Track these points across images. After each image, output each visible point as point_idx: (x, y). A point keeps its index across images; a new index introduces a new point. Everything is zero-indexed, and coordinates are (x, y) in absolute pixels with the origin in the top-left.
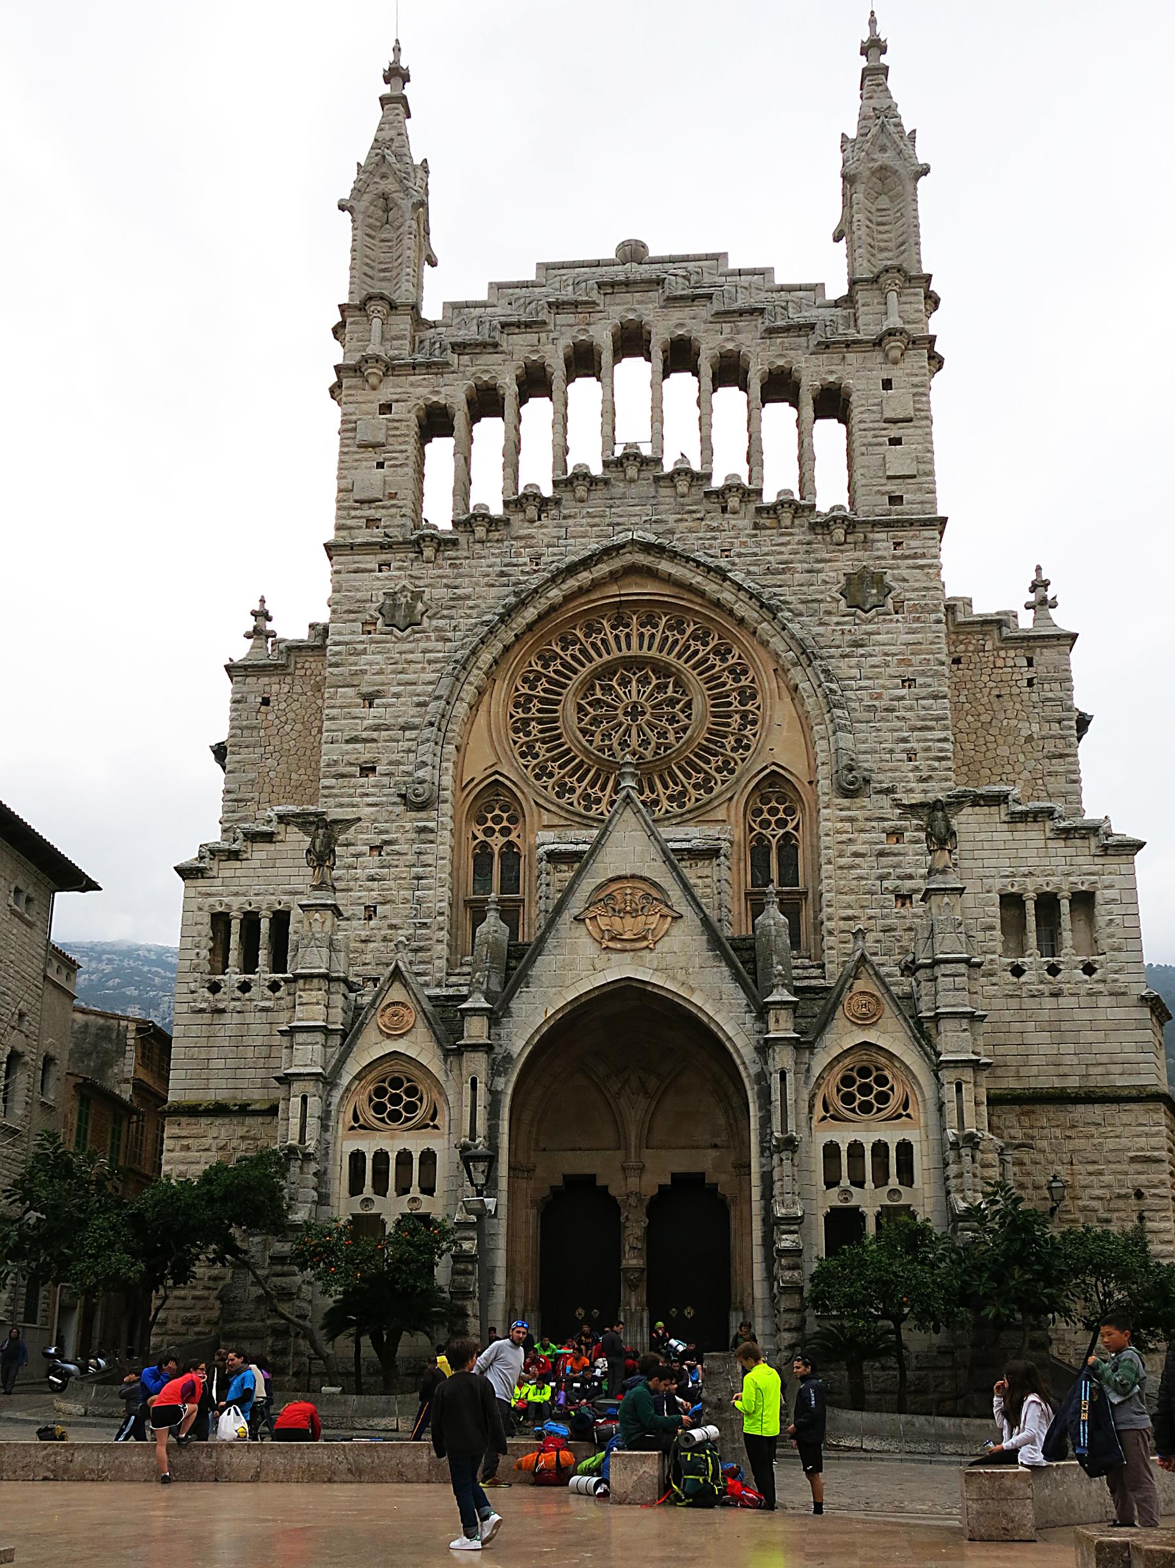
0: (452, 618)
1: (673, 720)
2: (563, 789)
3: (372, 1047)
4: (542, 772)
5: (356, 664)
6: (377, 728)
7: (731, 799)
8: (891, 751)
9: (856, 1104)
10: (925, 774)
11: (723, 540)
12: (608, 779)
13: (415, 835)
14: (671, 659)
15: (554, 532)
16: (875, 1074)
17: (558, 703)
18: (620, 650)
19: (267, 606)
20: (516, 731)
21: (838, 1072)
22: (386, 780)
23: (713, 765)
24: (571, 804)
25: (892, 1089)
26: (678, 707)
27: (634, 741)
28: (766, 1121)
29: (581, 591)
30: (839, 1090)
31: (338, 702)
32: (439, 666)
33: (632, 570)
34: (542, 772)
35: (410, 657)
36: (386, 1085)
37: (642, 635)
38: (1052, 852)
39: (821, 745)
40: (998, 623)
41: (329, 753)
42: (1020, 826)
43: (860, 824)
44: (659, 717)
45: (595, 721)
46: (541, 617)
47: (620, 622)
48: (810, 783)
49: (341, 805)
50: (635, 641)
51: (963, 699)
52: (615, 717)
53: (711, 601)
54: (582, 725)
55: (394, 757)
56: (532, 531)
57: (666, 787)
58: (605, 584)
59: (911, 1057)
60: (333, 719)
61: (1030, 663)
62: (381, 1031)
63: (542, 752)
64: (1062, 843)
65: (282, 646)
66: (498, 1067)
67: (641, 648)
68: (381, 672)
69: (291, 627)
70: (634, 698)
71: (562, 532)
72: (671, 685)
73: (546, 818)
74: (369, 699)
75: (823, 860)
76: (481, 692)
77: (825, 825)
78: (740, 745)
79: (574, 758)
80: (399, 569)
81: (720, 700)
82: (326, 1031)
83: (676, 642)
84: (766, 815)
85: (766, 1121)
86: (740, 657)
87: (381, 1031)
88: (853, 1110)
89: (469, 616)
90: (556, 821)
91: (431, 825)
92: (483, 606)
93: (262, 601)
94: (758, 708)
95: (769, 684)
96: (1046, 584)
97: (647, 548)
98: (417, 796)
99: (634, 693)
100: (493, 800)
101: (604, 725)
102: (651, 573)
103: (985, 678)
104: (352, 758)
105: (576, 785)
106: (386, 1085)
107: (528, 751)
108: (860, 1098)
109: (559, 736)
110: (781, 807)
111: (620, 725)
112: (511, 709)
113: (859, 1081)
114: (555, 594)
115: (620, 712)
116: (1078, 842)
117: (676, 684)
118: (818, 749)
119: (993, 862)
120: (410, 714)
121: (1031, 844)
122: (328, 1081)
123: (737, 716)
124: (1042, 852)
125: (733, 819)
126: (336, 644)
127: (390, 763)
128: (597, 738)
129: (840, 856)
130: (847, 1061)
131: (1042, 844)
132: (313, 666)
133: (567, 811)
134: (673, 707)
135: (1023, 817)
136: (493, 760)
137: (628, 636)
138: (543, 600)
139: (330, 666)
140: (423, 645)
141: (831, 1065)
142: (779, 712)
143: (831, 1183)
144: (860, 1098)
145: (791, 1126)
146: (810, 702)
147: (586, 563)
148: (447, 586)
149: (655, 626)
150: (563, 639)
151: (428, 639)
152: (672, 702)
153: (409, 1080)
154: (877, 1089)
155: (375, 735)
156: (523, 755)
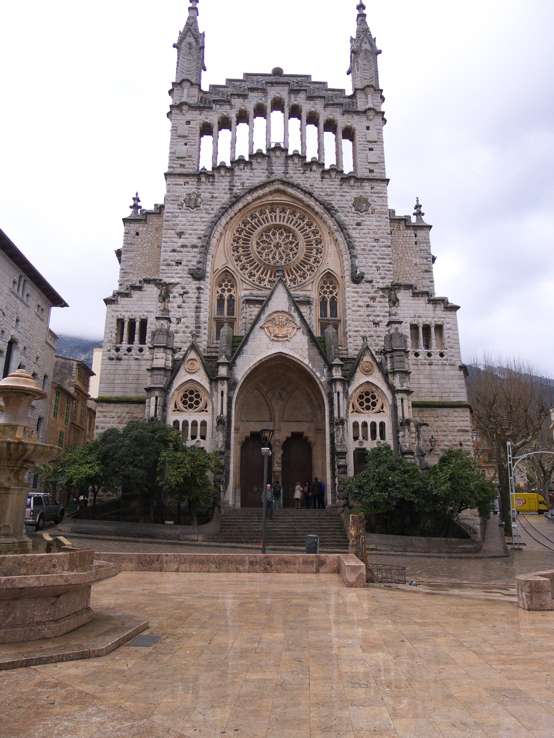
0: (211, 205)
1: (291, 250)
2: (251, 275)
3: (182, 377)
4: (243, 268)
5: (175, 221)
6: (183, 246)
7: (313, 282)
8: (371, 267)
9: (364, 406)
10: (383, 276)
11: (311, 181)
12: (267, 272)
13: (196, 291)
14: (291, 226)
15: (249, 174)
16: (371, 394)
17: (249, 241)
18: (272, 221)
19: (138, 196)
20: (234, 251)
22: (185, 268)
23: (306, 268)
24: (254, 281)
25: (377, 401)
26: (294, 245)
27: (277, 257)
28: (332, 412)
29: (259, 198)
30: (358, 401)
31: (168, 236)
32: (206, 224)
33: (278, 191)
34: (243, 268)
35: (195, 219)
36: (188, 393)
37: (280, 216)
39: (346, 263)
40: (405, 220)
41: (164, 256)
42: (417, 298)
43: (361, 294)
44: (286, 249)
45: (263, 249)
46: (244, 207)
47: (272, 211)
48: (342, 277)
49: (168, 277)
50: (278, 218)
52: (270, 247)
53: (306, 205)
54: (258, 250)
55: (190, 259)
56: (241, 173)
57: (289, 276)
59: (384, 388)
60: (166, 242)
61: (416, 236)
62: (186, 371)
63: (243, 260)
65: (144, 212)
66: (232, 386)
67: (280, 221)
68: (184, 225)
69: (148, 205)
70: (278, 240)
71: (252, 175)
72: (291, 237)
73: (245, 286)
74: (180, 235)
75: (347, 307)
76: (221, 235)
77: (348, 294)
78: (316, 261)
79: (255, 263)
80: (192, 185)
81: (309, 243)
83: (293, 220)
84: (325, 289)
85: (332, 412)
86: (316, 227)
87: (186, 371)
88: (363, 409)
89: (218, 205)
90: (249, 287)
91: (202, 286)
92: (223, 201)
93: (137, 194)
94: (322, 247)
95: (327, 238)
96: (420, 206)
97: (283, 182)
98: (198, 275)
99: (278, 238)
100: (226, 278)
101: (266, 251)
102: (284, 193)
103: (400, 240)
104: (173, 258)
105: (256, 273)
106: (188, 393)
107: (238, 259)
108: (366, 404)
109: (250, 254)
110: (331, 286)
111: (272, 251)
112: (232, 242)
113: (365, 397)
115: (272, 245)
117: (293, 236)
118: (345, 264)
119: (407, 312)
120: (195, 241)
121: (421, 305)
122: (166, 390)
123: (315, 250)
124: (425, 308)
125: (314, 290)
126: (167, 213)
127: (187, 261)
128: (264, 255)
129: (353, 306)
131: (424, 305)
132: (156, 220)
133: (253, 284)
134: (292, 245)
136: (225, 262)
137: (275, 216)
138: (245, 200)
139: (165, 221)
140: (200, 215)
141: (355, 390)
142: (330, 249)
143: (356, 438)
144: (366, 404)
145: (342, 415)
146: (342, 246)
148: (210, 193)
149: (285, 213)
150: (251, 216)
151: (202, 213)
152: (291, 243)
153: (196, 391)
154: (372, 400)
155: (182, 249)
156: (236, 260)
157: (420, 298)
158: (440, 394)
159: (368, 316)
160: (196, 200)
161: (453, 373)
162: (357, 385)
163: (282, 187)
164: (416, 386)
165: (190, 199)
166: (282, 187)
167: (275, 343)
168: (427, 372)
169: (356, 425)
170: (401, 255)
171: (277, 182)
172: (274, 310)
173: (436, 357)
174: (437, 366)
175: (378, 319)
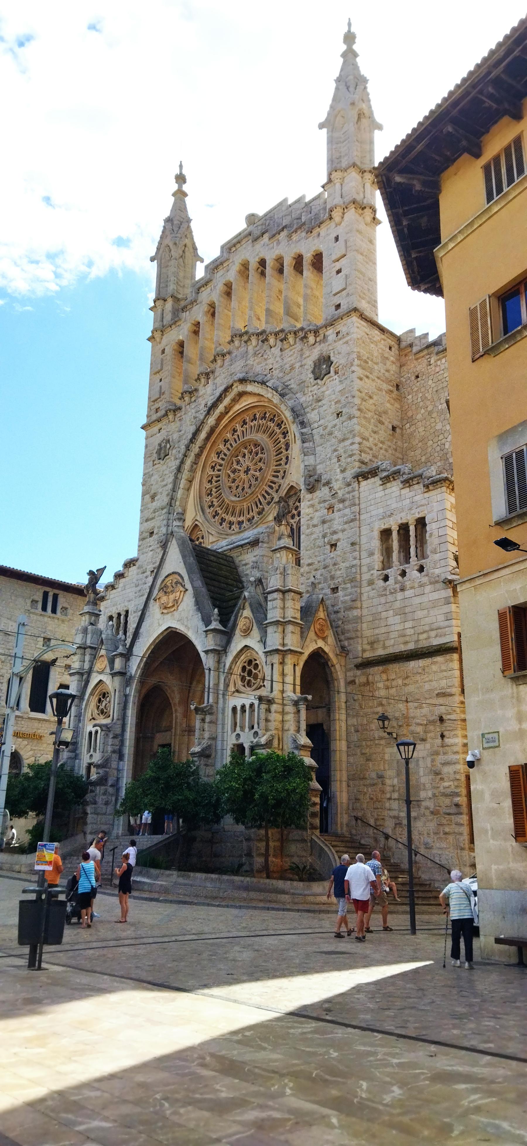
38: (403, 497)
42: (388, 485)
58: (232, 407)
64: (408, 490)
82: (82, 674)
103: (430, 382)
114: (211, 421)
116: (416, 487)
130: (242, 658)
135: (386, 480)
157: (394, 483)
158: (415, 638)
159: (324, 537)
160: (165, 447)
161: (435, 596)
162: (234, 653)
163: (241, 388)
164: (383, 630)
165: (161, 449)
166: (241, 388)
167: (166, 616)
168: (398, 605)
171: (235, 385)
173: (413, 573)
174: (412, 591)
175: (335, 537)
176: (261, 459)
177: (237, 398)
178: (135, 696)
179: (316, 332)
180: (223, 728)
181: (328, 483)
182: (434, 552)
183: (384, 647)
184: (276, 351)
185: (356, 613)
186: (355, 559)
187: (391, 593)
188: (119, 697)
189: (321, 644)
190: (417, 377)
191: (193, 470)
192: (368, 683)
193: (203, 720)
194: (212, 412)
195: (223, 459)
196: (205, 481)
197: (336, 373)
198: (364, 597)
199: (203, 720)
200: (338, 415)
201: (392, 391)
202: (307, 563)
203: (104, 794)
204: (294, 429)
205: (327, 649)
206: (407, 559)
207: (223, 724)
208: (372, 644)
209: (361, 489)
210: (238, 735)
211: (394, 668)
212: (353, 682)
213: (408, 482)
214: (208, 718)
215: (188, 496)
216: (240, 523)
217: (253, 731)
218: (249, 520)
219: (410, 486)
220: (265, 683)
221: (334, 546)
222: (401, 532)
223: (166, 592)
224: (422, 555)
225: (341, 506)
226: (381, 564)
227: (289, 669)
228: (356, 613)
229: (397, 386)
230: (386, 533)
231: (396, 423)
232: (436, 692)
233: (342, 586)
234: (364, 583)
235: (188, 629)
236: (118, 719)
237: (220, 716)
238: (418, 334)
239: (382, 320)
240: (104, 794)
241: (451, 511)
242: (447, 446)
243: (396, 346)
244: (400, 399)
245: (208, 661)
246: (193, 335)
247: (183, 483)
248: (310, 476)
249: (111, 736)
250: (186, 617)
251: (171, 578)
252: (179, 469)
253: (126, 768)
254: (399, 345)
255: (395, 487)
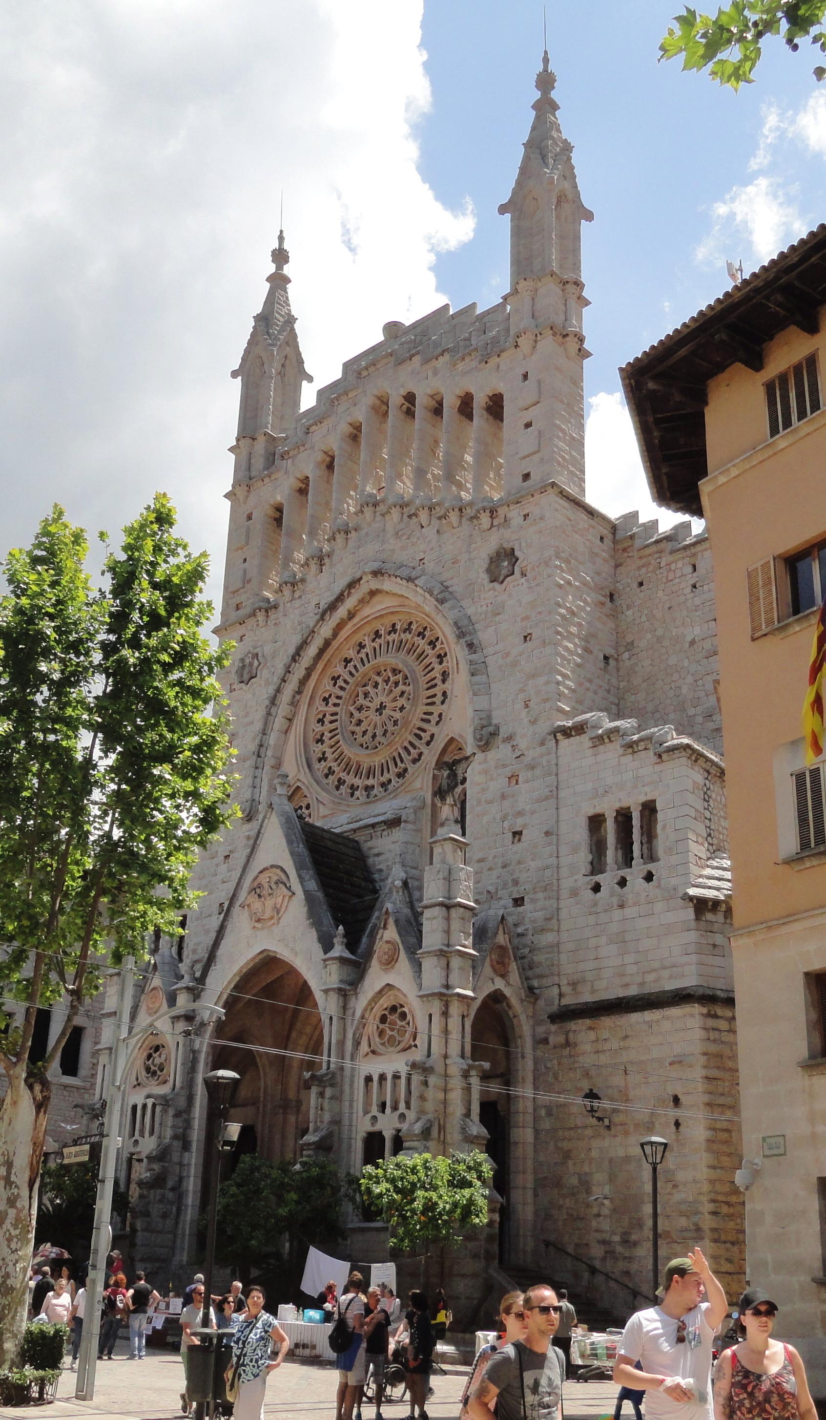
21: (378, 1011)
33: (373, 593)
42: (601, 748)
51: (644, 619)
114: (326, 631)
147: (340, 599)
157: (610, 746)
158: (639, 979)
159: (504, 819)
160: (251, 664)
164: (590, 965)
165: (244, 667)
166: (374, 584)
169: (369, 1079)
170: (660, 632)
172: (261, 868)
174: (635, 909)
176: (403, 693)
177: (368, 598)
178: (208, 1054)
179: (493, 512)
180: (351, 1106)
181: (509, 738)
182: (669, 851)
183: (593, 991)
184: (430, 532)
185: (549, 938)
186: (551, 856)
187: (606, 911)
188: (185, 1052)
189: (499, 984)
190: (641, 584)
191: (294, 704)
192: (567, 1044)
193: (321, 1094)
194: (327, 617)
195: (342, 688)
196: (313, 720)
197: (523, 575)
198: (563, 914)
199: (321, 1094)
200: (525, 637)
201: (603, 604)
202: (476, 858)
203: (161, 1201)
204: (457, 652)
205: (507, 992)
206: (628, 860)
207: (351, 1101)
208: (574, 985)
209: (561, 751)
210: (374, 1118)
211: (607, 1022)
212: (545, 1041)
213: (631, 747)
214: (329, 1092)
215: (285, 742)
216: (368, 789)
217: (398, 1113)
218: (383, 785)
219: (634, 752)
220: (417, 1042)
221: (517, 834)
222: (620, 819)
223: (259, 896)
224: (651, 857)
225: (529, 774)
226: (589, 867)
227: (454, 1023)
228: (549, 938)
229: (611, 596)
230: (596, 822)
231: (610, 651)
232: (669, 1060)
233: (532, 896)
234: (564, 894)
235: (296, 954)
236: (182, 1088)
237: (347, 1088)
238: (642, 520)
239: (592, 499)
240: (161, 1201)
241: (693, 793)
242: (684, 690)
243: (610, 536)
244: (614, 615)
245: (327, 1006)
246: (297, 495)
247: (279, 723)
248: (483, 727)
249: (171, 1112)
250: (289, 933)
251: (267, 874)
252: (273, 701)
253: (193, 1161)
254: (614, 534)
255: (612, 752)
